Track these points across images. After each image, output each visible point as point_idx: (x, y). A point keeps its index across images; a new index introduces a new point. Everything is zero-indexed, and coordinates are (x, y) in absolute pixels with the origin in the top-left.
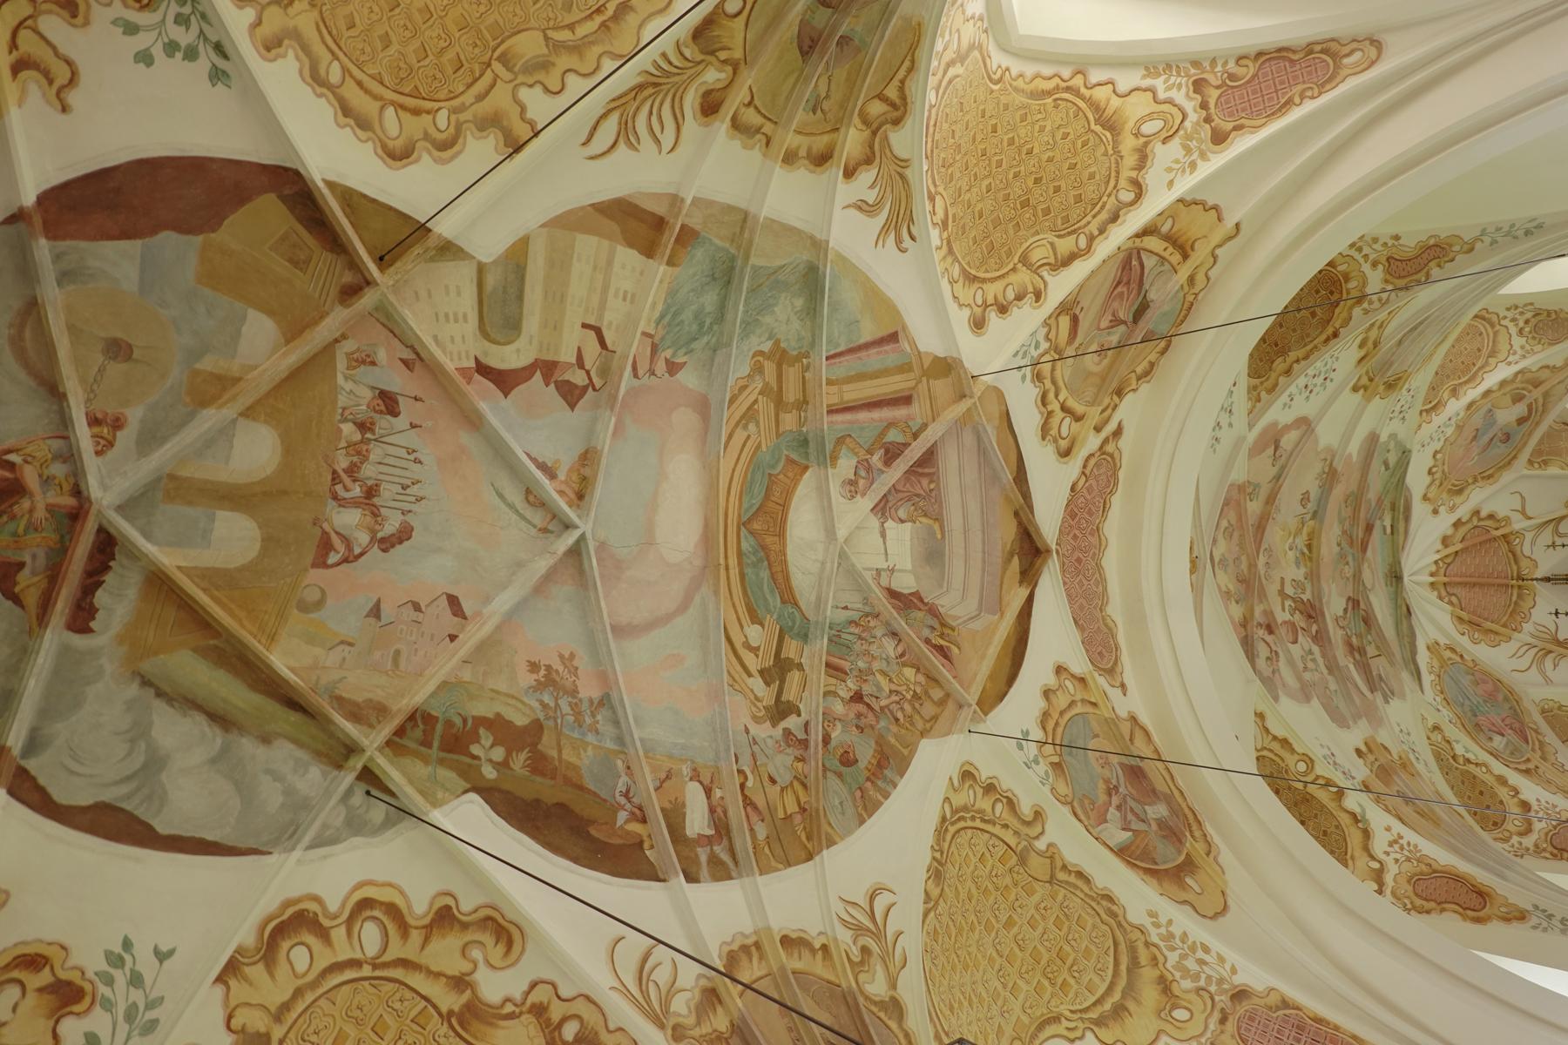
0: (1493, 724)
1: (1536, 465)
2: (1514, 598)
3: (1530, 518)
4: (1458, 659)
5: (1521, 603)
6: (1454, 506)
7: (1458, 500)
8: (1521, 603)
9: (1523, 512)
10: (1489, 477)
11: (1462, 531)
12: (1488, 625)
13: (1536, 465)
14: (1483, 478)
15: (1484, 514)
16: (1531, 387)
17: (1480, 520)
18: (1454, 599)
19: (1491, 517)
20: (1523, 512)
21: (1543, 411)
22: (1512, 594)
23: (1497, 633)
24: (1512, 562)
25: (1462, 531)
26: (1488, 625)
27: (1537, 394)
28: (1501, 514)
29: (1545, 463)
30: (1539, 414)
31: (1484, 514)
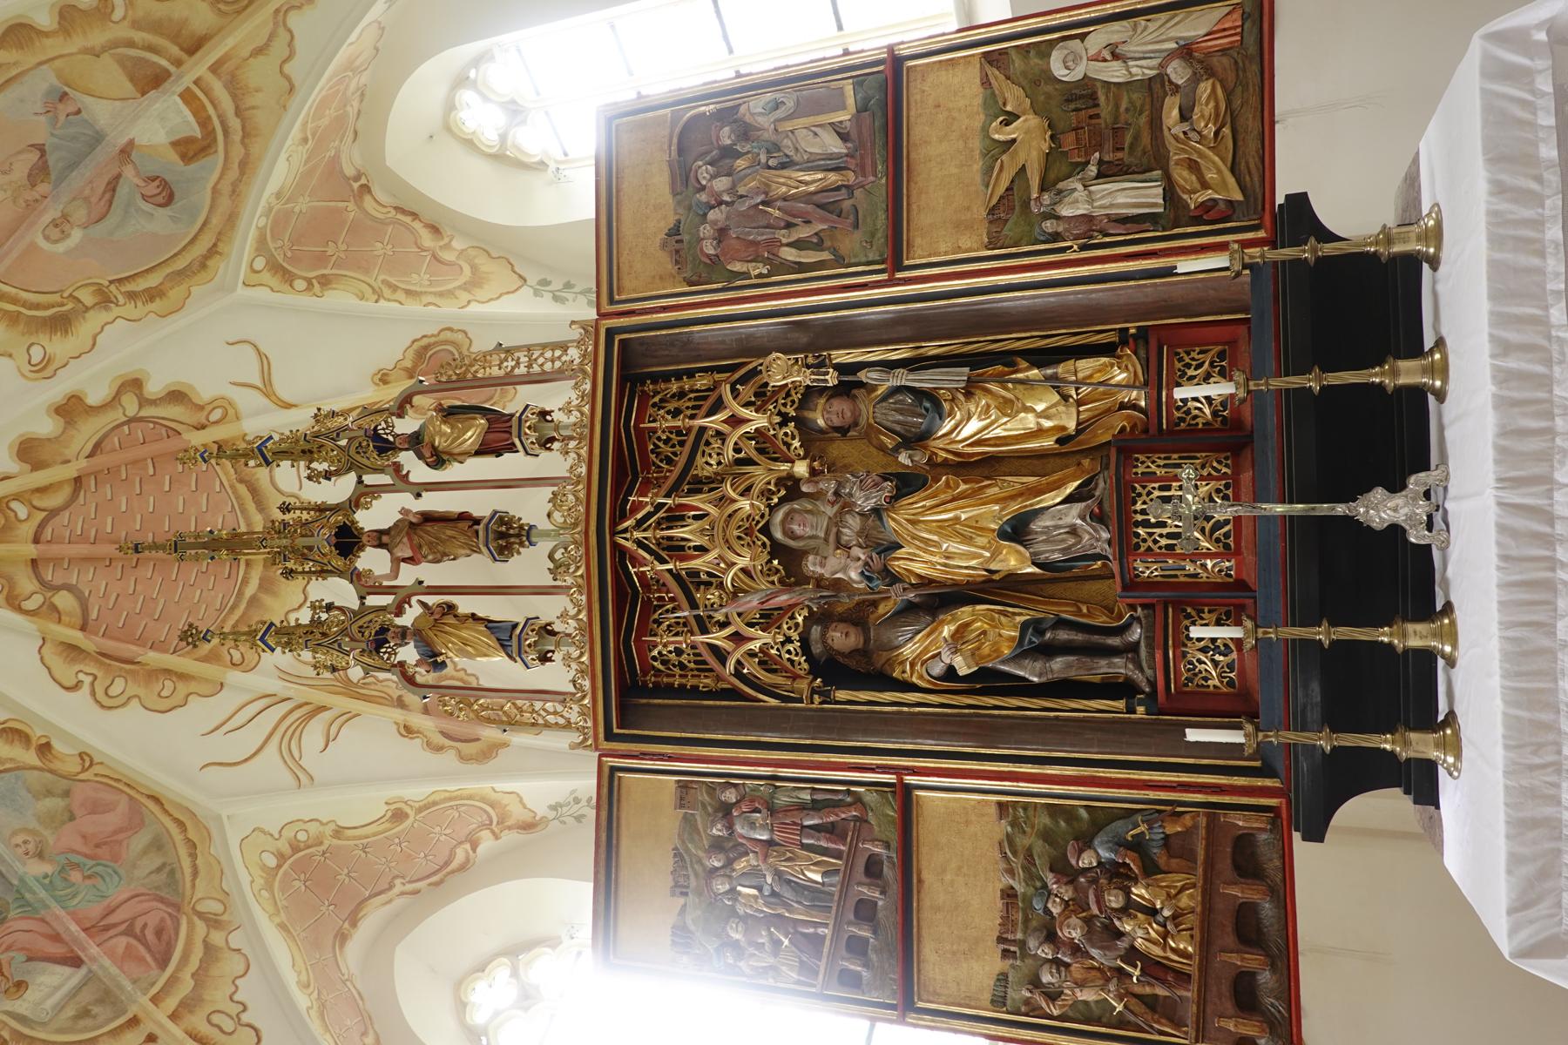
0: (56, 938)
1: (300, 284)
2: (250, 590)
3: (288, 406)
4: (31, 757)
5: (267, 600)
6: (47, 361)
7: (59, 346)
8: (267, 600)
9: (267, 389)
10: (152, 295)
11: (88, 431)
12: (153, 658)
13: (300, 284)
14: (132, 296)
15: (154, 388)
16: (175, 50)
17: (144, 402)
18: (64, 600)
19: (177, 396)
20: (267, 389)
21: (246, 135)
22: (245, 581)
23: (183, 677)
24: (251, 507)
25: (88, 431)
26: (153, 658)
27: (199, 67)
28: (205, 391)
29: (325, 282)
30: (237, 137)
31: (154, 388)
